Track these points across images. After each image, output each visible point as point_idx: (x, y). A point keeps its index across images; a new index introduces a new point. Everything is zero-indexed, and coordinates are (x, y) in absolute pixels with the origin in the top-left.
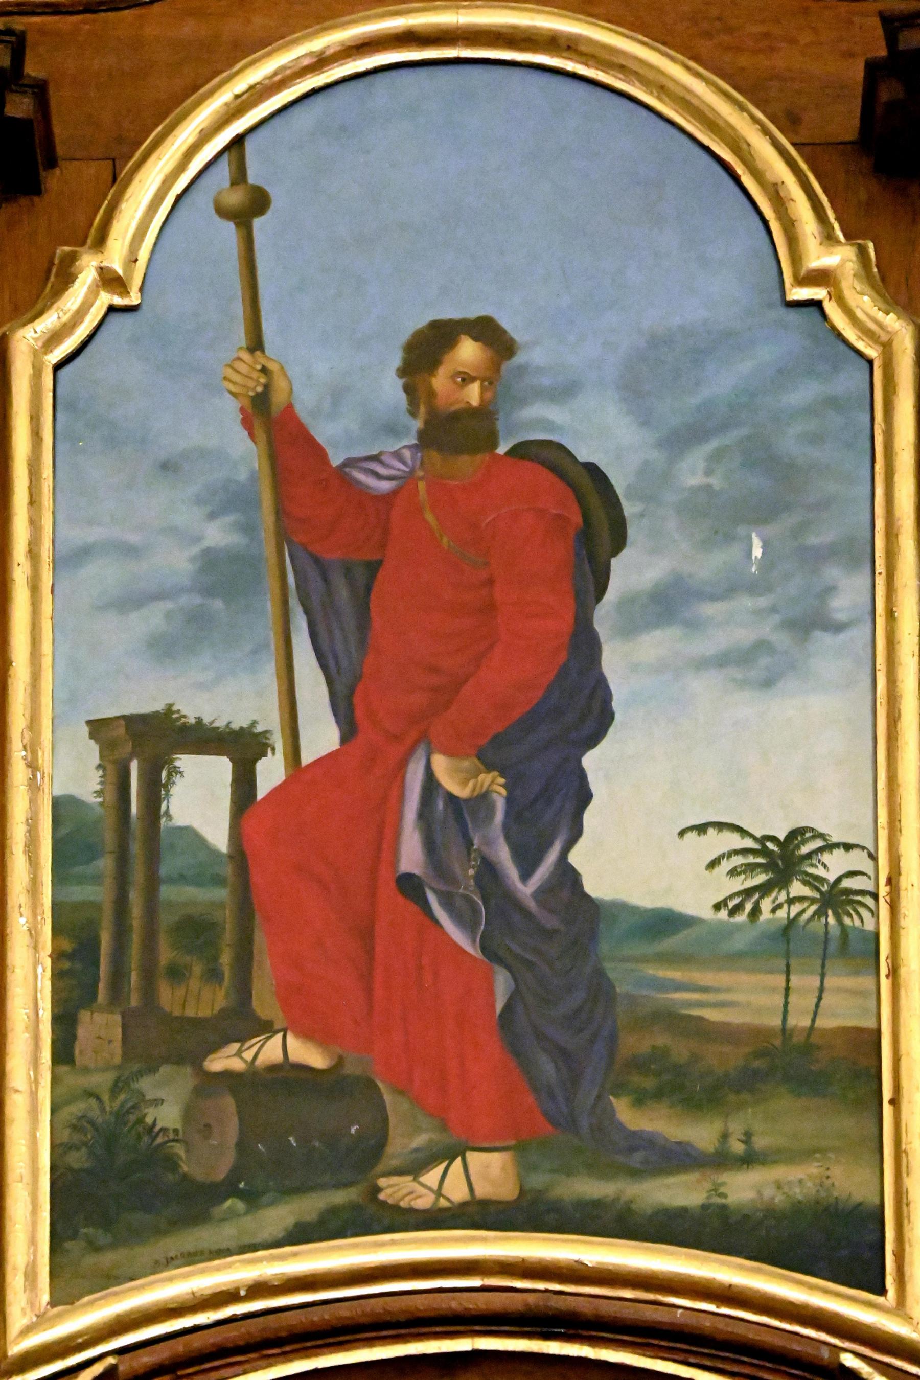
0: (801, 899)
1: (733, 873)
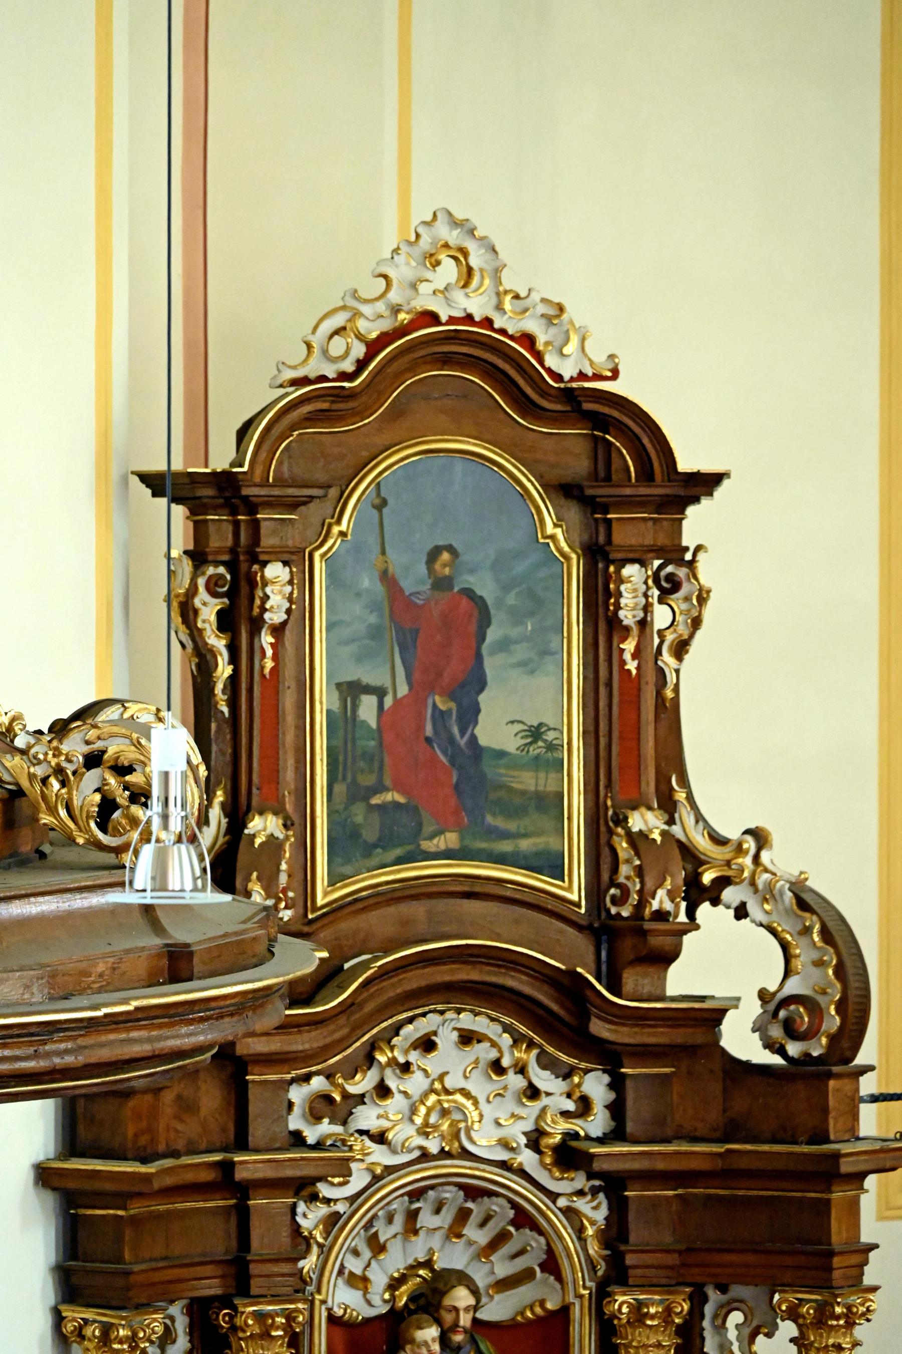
0: (541, 747)
1: (522, 738)
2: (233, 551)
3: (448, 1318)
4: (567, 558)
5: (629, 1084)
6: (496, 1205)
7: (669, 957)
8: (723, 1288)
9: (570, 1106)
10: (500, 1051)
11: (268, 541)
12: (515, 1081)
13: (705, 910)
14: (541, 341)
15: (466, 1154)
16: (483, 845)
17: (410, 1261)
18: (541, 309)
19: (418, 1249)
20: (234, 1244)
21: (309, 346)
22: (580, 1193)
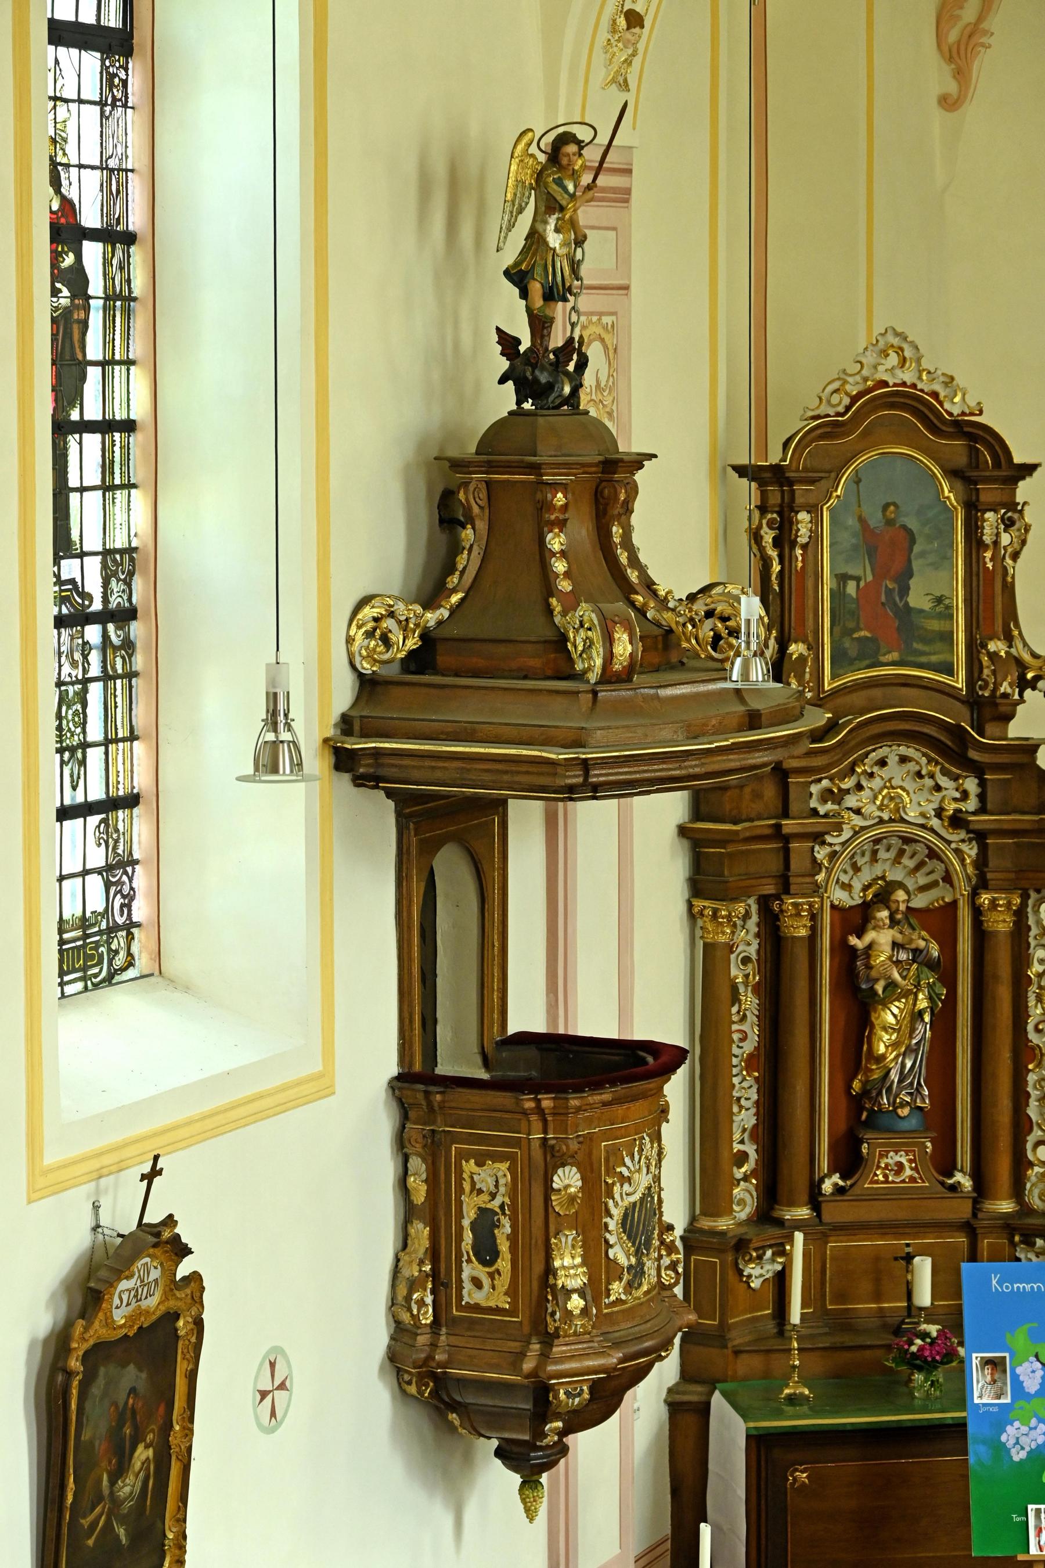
2: (781, 506)
3: (894, 906)
4: (956, 509)
5: (989, 784)
6: (919, 847)
7: (1009, 717)
8: (1038, 891)
9: (957, 795)
10: (921, 766)
11: (799, 500)
12: (929, 782)
13: (1028, 693)
14: (942, 395)
15: (903, 820)
16: (912, 659)
17: (874, 876)
18: (942, 379)
19: (878, 870)
20: (782, 867)
21: (820, 399)
22: (963, 841)
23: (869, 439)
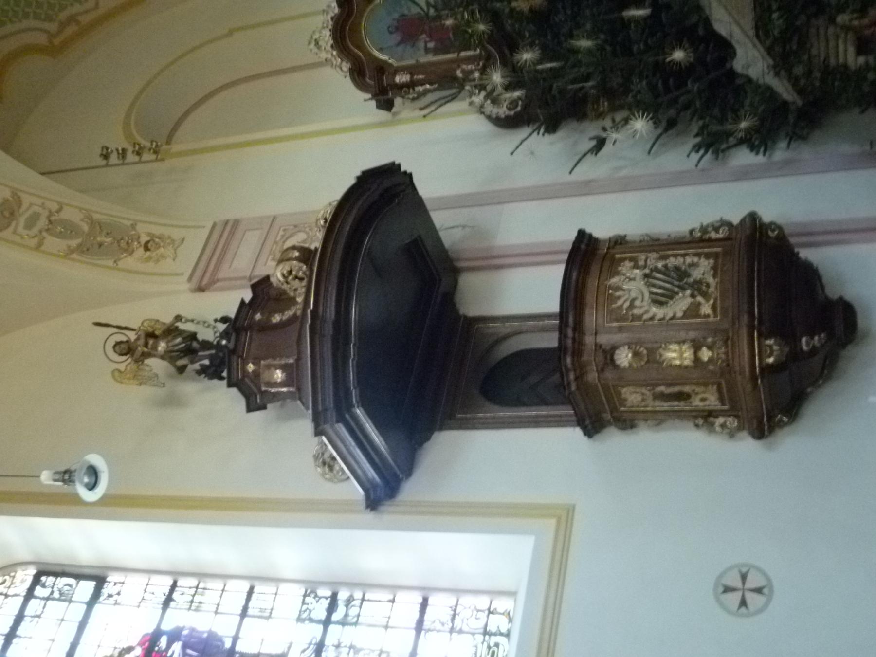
23: (361, 47)
